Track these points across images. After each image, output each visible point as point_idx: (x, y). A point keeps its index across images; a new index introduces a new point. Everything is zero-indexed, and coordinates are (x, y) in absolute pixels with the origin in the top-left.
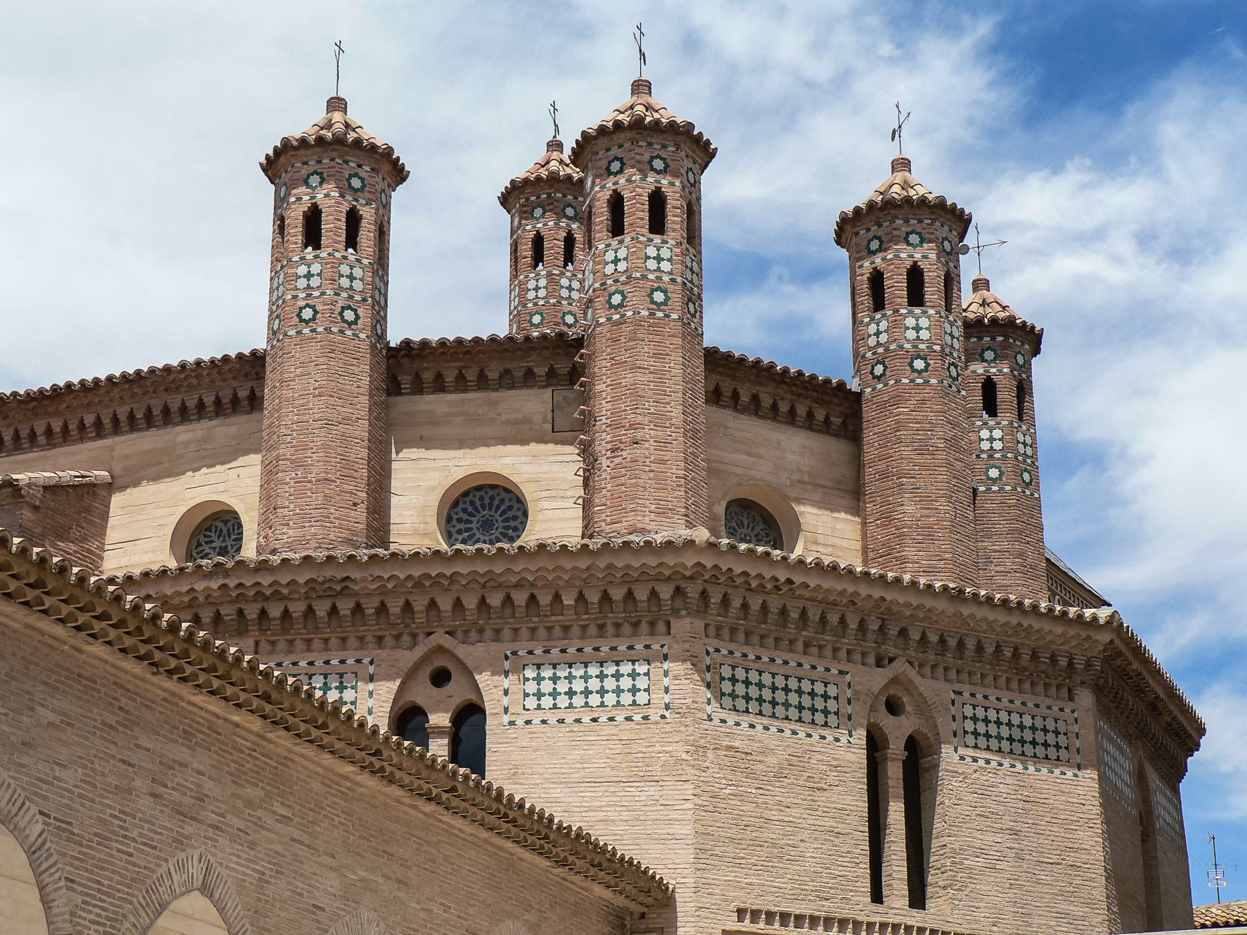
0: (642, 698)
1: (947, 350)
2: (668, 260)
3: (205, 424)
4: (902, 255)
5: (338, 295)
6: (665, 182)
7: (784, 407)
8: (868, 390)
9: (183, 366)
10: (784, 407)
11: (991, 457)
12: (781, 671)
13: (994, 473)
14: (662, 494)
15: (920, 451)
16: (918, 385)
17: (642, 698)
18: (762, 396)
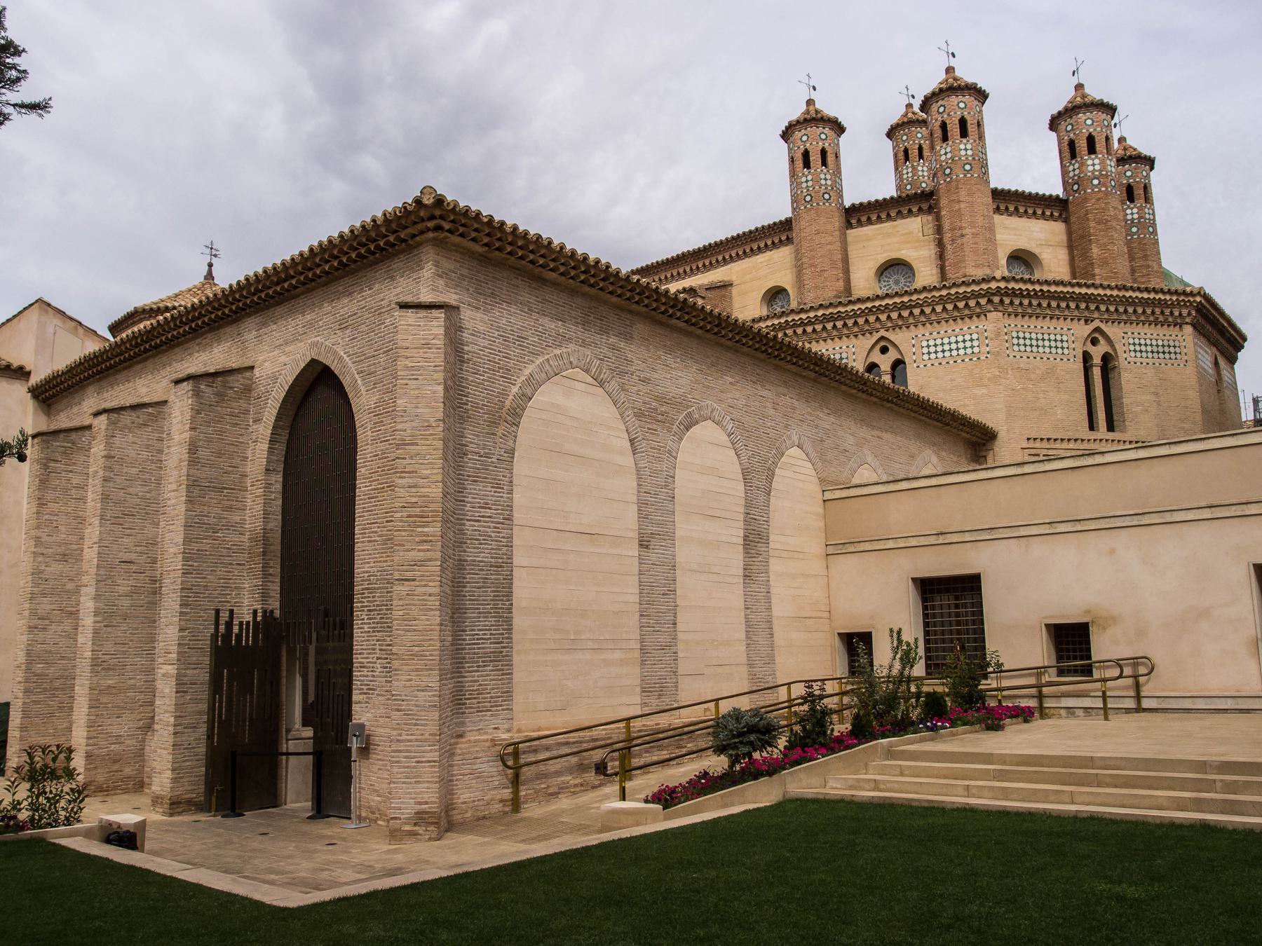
0: (976, 350)
3: (768, 253)
7: (1030, 211)
9: (757, 229)
13: (1134, 230)
15: (1099, 223)
17: (976, 350)
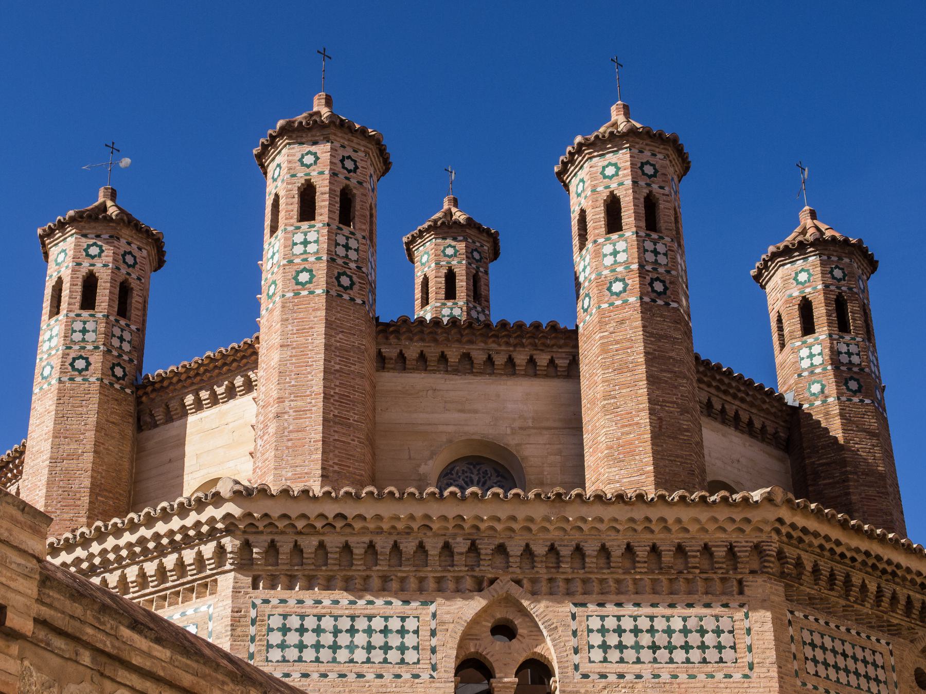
2: (316, 242)
4: (599, 189)
5: (70, 348)
6: (314, 174)
7: (500, 360)
8: (581, 325)
10: (500, 360)
11: (812, 373)
12: (347, 612)
14: (298, 461)
15: (620, 371)
16: (617, 306)
18: (474, 354)
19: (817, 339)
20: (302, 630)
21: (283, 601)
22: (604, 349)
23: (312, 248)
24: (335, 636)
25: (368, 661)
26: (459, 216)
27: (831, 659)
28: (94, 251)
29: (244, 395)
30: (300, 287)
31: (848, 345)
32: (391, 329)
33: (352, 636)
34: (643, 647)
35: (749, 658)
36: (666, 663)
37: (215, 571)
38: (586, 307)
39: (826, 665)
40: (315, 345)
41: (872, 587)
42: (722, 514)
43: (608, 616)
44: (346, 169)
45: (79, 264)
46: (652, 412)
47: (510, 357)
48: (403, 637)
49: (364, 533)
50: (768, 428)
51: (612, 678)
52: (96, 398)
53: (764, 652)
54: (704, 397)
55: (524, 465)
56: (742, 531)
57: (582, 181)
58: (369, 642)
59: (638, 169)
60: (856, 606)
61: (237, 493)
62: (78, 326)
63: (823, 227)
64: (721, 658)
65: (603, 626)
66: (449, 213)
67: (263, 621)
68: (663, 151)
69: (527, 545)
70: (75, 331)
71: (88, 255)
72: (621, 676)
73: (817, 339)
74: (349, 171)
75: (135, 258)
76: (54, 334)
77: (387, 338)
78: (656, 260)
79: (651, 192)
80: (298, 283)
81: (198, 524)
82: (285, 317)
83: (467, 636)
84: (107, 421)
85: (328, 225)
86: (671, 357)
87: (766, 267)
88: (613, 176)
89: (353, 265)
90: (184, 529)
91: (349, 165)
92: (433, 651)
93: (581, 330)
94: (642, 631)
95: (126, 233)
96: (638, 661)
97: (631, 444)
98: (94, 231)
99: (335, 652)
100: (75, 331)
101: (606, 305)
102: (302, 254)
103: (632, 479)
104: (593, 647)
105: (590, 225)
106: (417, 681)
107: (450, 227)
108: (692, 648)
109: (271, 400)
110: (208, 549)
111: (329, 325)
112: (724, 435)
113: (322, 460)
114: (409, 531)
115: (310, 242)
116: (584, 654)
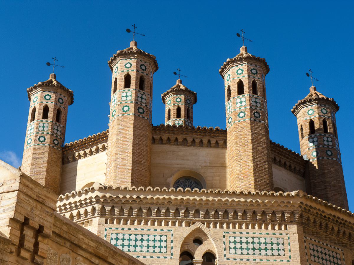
1: (253, 108)
5: (38, 133)
6: (130, 71)
7: (197, 141)
8: (228, 129)
10: (197, 141)
12: (140, 233)
16: (242, 122)
18: (188, 138)
19: (315, 135)
20: (123, 239)
21: (117, 229)
22: (236, 138)
23: (129, 98)
24: (136, 242)
25: (148, 251)
26: (182, 87)
27: (320, 256)
28: (48, 97)
29: (102, 152)
30: (124, 112)
31: (327, 138)
32: (157, 129)
33: (142, 242)
34: (250, 249)
35: (289, 254)
36: (258, 255)
37: (91, 217)
38: (230, 122)
39: (318, 257)
40: (129, 134)
41: (336, 229)
42: (279, 200)
43: (237, 237)
44: (142, 69)
45: (42, 102)
46: (254, 161)
47: (201, 140)
48: (161, 243)
49: (147, 204)
50: (297, 168)
51: (238, 260)
52: (47, 152)
53: (295, 252)
54: (273, 156)
55: (205, 180)
56: (287, 206)
57: (229, 75)
58: (148, 245)
59: (250, 72)
60: (330, 236)
61: (100, 188)
62: (41, 125)
63: (318, 94)
64: (279, 254)
65: (235, 240)
66: (178, 86)
67: (109, 236)
68: (260, 65)
69: (207, 210)
70: (40, 127)
71: (45, 99)
72: (242, 260)
73: (315, 135)
74: (143, 70)
75: (63, 100)
76: (32, 128)
77: (156, 132)
78: (256, 105)
79: (254, 80)
80: (124, 111)
81: (86, 199)
82: (119, 123)
83: (184, 244)
84: (52, 160)
85: (135, 90)
86: (261, 141)
87: (297, 108)
88: (241, 73)
89: (144, 105)
90: (80, 201)
91: (143, 67)
92: (172, 248)
93: (228, 131)
94: (249, 243)
95: (60, 91)
96: (248, 254)
97: (246, 173)
98: (48, 90)
99: (135, 248)
100: (40, 127)
101: (237, 121)
102: (125, 100)
103: (246, 186)
104: (231, 248)
105: (232, 92)
106: (166, 259)
107: (179, 91)
108: (268, 249)
109: (113, 154)
110: (89, 209)
111: (135, 127)
112: (280, 171)
113: (131, 176)
114: (163, 204)
115: (128, 96)
116: (228, 250)
